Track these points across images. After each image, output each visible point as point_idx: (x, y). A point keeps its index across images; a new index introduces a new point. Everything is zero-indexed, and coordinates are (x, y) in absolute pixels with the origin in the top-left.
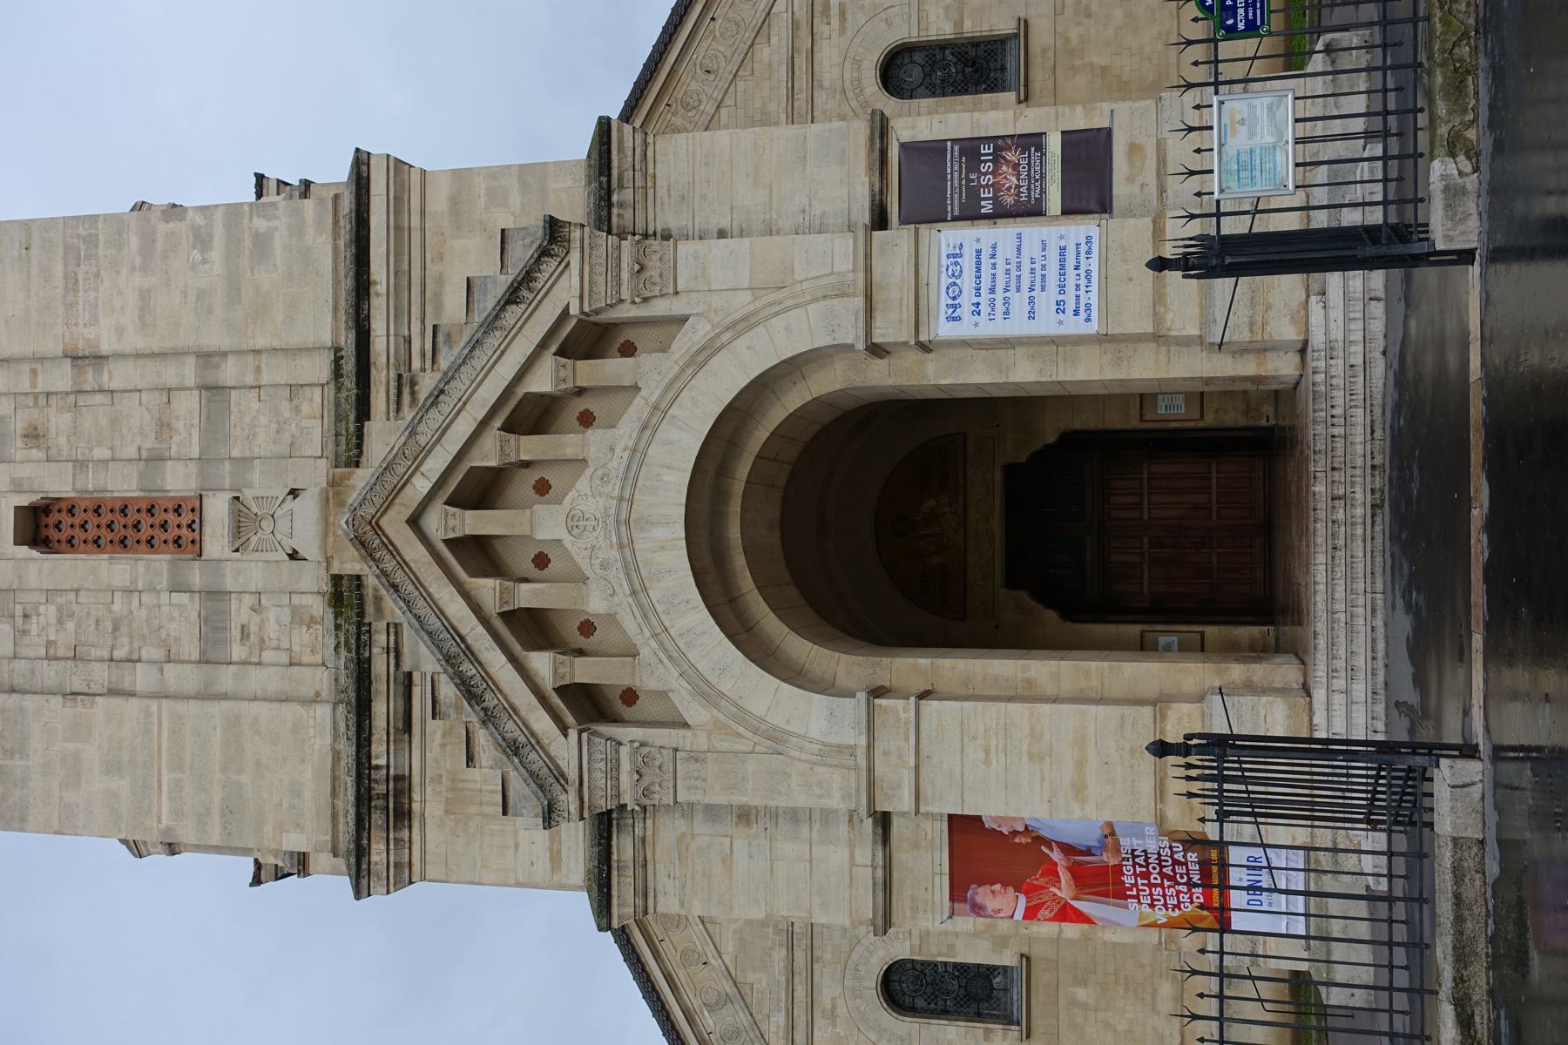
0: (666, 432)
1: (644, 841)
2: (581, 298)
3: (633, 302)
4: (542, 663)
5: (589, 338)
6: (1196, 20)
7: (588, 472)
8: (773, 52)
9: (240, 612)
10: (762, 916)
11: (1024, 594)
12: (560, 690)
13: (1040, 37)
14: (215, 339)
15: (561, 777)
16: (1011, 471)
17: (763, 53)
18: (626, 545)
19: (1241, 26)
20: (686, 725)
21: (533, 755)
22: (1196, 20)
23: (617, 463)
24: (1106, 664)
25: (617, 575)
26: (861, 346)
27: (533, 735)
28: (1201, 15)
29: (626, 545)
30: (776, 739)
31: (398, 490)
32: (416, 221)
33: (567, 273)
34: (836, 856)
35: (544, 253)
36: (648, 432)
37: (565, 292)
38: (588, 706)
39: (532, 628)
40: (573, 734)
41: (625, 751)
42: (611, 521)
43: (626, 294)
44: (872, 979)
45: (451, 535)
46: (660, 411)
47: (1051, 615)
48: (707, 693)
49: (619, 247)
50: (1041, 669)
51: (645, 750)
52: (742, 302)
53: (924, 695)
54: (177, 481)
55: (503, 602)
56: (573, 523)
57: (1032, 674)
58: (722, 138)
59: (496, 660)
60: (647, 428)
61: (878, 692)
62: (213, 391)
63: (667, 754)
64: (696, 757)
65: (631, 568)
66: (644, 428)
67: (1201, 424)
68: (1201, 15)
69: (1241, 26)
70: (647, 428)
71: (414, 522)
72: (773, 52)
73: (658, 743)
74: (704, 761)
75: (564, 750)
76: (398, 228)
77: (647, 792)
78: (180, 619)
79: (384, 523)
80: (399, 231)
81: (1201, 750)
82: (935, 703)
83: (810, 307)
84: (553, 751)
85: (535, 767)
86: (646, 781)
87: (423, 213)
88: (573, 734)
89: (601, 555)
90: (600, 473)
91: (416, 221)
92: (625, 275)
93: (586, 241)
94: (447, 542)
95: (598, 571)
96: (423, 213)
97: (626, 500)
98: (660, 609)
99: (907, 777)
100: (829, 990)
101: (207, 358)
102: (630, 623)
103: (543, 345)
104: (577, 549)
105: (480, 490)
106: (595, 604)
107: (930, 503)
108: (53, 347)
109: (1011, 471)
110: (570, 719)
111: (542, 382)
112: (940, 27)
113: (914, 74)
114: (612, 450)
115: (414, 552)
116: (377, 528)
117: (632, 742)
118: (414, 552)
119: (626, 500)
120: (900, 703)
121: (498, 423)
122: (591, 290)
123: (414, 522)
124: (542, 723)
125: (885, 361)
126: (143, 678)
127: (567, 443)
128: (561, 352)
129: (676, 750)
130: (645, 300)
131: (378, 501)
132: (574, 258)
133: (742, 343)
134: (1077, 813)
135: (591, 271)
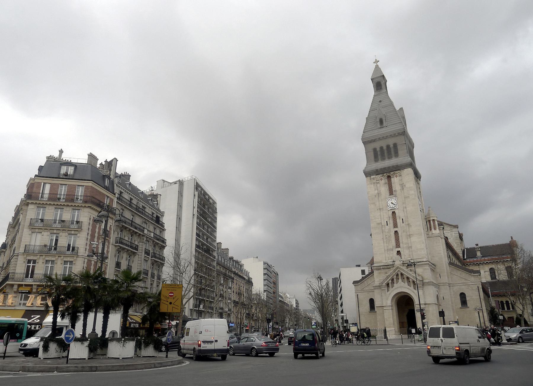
4: (390, 281)
8: (463, 281)
9: (391, 252)
13: (467, 309)
17: (463, 280)
30: (387, 299)
39: (393, 280)
48: (390, 294)
54: (401, 245)
72: (463, 281)
75: (384, 284)
80: (422, 264)
101: (411, 247)
105: (402, 274)
111: (410, 280)
112: (467, 299)
113: (463, 296)
115: (397, 271)
118: (397, 271)
126: (385, 244)
127: (406, 282)
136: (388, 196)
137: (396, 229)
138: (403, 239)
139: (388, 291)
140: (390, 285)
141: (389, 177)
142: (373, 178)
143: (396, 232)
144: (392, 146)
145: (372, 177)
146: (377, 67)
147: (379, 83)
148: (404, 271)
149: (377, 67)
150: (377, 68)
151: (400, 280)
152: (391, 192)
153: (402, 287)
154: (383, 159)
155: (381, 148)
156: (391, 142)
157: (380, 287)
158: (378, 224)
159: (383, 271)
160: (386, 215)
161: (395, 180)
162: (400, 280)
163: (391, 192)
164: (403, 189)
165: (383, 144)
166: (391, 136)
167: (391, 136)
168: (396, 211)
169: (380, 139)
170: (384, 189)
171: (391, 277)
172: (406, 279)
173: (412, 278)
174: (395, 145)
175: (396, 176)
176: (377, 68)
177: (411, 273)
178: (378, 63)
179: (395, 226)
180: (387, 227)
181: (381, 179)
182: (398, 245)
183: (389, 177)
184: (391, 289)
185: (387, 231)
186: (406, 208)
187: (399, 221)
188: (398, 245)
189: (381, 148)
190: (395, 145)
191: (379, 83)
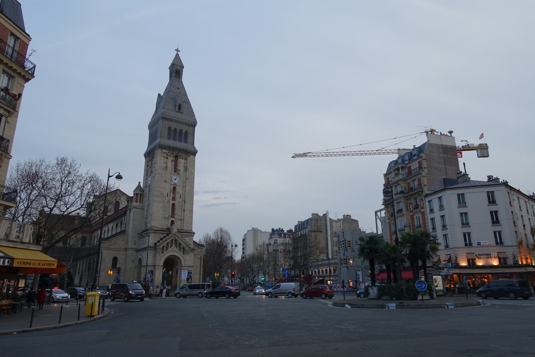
5: (184, 248)
14: (185, 221)
30: (160, 260)
37: (187, 248)
44: (116, 256)
48: (164, 255)
54: (176, 217)
62: (181, 220)
78: (167, 216)
100: (115, 252)
105: (176, 241)
108: (185, 208)
111: (182, 246)
136: (173, 172)
137: (174, 202)
138: (178, 211)
139: (162, 252)
140: (165, 248)
141: (176, 157)
142: (164, 153)
143: (173, 204)
144: (184, 132)
145: (164, 151)
146: (177, 55)
147: (176, 70)
148: (178, 237)
149: (177, 55)
150: (177, 57)
151: (174, 246)
152: (176, 170)
153: (173, 251)
154: (175, 139)
155: (181, 131)
156: (184, 128)
158: (161, 193)
159: (158, 235)
160: (168, 188)
161: (181, 162)
162: (174, 246)
163: (176, 170)
164: (186, 171)
165: (179, 127)
166: (186, 124)
167: (186, 124)
168: (177, 187)
169: (176, 121)
170: (170, 165)
172: (178, 245)
174: (186, 132)
175: (182, 159)
176: (177, 57)
177: (170, 240)
178: (179, 53)
179: (174, 199)
180: (167, 198)
181: (170, 156)
182: (173, 215)
183: (176, 157)
184: (165, 252)
185: (166, 201)
186: (185, 187)
187: (178, 196)
188: (173, 215)
189: (175, 129)
190: (186, 132)
191: (176, 70)
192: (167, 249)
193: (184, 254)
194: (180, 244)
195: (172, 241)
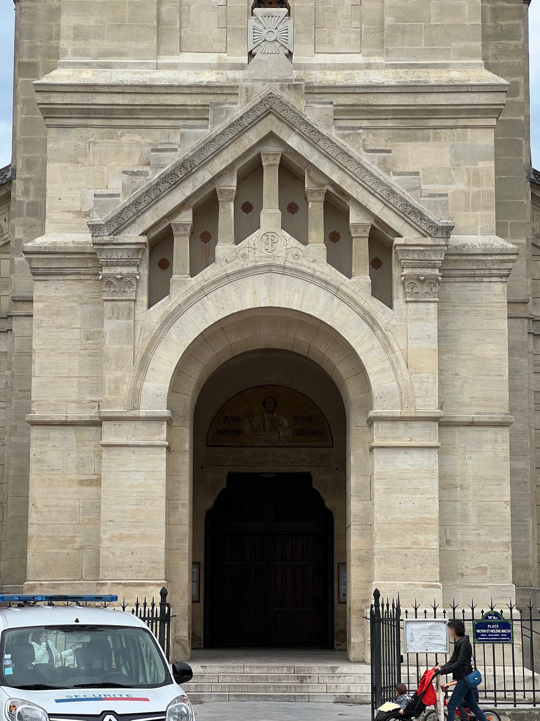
0: (324, 296)
1: (79, 274)
2: (405, 245)
3: (402, 276)
5: (381, 243)
6: (482, 612)
7: (301, 246)
10: (34, 347)
11: (224, 486)
12: (169, 228)
15: (116, 232)
16: (307, 477)
18: (256, 270)
19: (478, 631)
20: (149, 306)
21: (131, 214)
22: (482, 612)
23: (305, 265)
24: (187, 551)
25: (240, 264)
26: (372, 414)
27: (142, 213)
28: (484, 614)
29: (256, 270)
31: (291, 127)
32: (462, 122)
33: (420, 236)
34: (71, 392)
35: (432, 225)
36: (324, 284)
37: (407, 236)
38: (159, 246)
39: (206, 207)
40: (144, 239)
41: (134, 270)
42: (270, 261)
43: (406, 272)
45: (263, 158)
46: (337, 292)
47: (210, 504)
48: (169, 320)
49: (434, 267)
50: (184, 513)
51: (134, 282)
52: (398, 344)
53: (168, 449)
55: (220, 191)
56: (270, 236)
57: (181, 509)
58: (504, 325)
59: (187, 190)
60: (326, 284)
61: (169, 421)
63: (134, 297)
64: (130, 314)
65: (242, 273)
66: (326, 282)
67: (336, 601)
68: (484, 614)
69: (478, 631)
70: (326, 284)
71: (271, 136)
73: (139, 292)
74: (129, 318)
75: (133, 235)
76: (458, 112)
77: (109, 284)
79: (271, 116)
81: (163, 610)
82: (165, 456)
83: (395, 384)
84: (135, 226)
85: (124, 215)
86: (115, 283)
87: (466, 127)
88: (144, 239)
89: (250, 254)
90: (301, 254)
91: (462, 122)
92: (418, 271)
93: (439, 248)
94: (259, 156)
95: (241, 252)
96: (466, 127)
97: (284, 270)
98: (218, 291)
99: (123, 441)
102: (209, 273)
103: (377, 220)
104: (253, 239)
105: (292, 172)
106: (223, 249)
107: (286, 423)
109: (307, 477)
110: (153, 234)
111: (354, 217)
114: (314, 261)
116: (268, 113)
117: (139, 274)
118: (252, 138)
119: (284, 270)
120: (164, 436)
121: (331, 189)
122: (409, 250)
123: (271, 136)
124: (149, 219)
125: (366, 425)
127: (317, 235)
128: (373, 227)
129: (135, 301)
130: (403, 283)
131: (284, 113)
132: (429, 241)
133: (376, 342)
134: (104, 537)
135: (420, 250)
139: (157, 292)
140: (182, 247)
148: (312, 136)
151: (270, 215)
153: (271, 274)
157: (87, 263)
162: (270, 215)
171: (204, 176)
172: (316, 209)
173: (368, 206)
184: (183, 284)
192: (202, 259)
193: (382, 291)
194: (336, 206)
195: (250, 173)
